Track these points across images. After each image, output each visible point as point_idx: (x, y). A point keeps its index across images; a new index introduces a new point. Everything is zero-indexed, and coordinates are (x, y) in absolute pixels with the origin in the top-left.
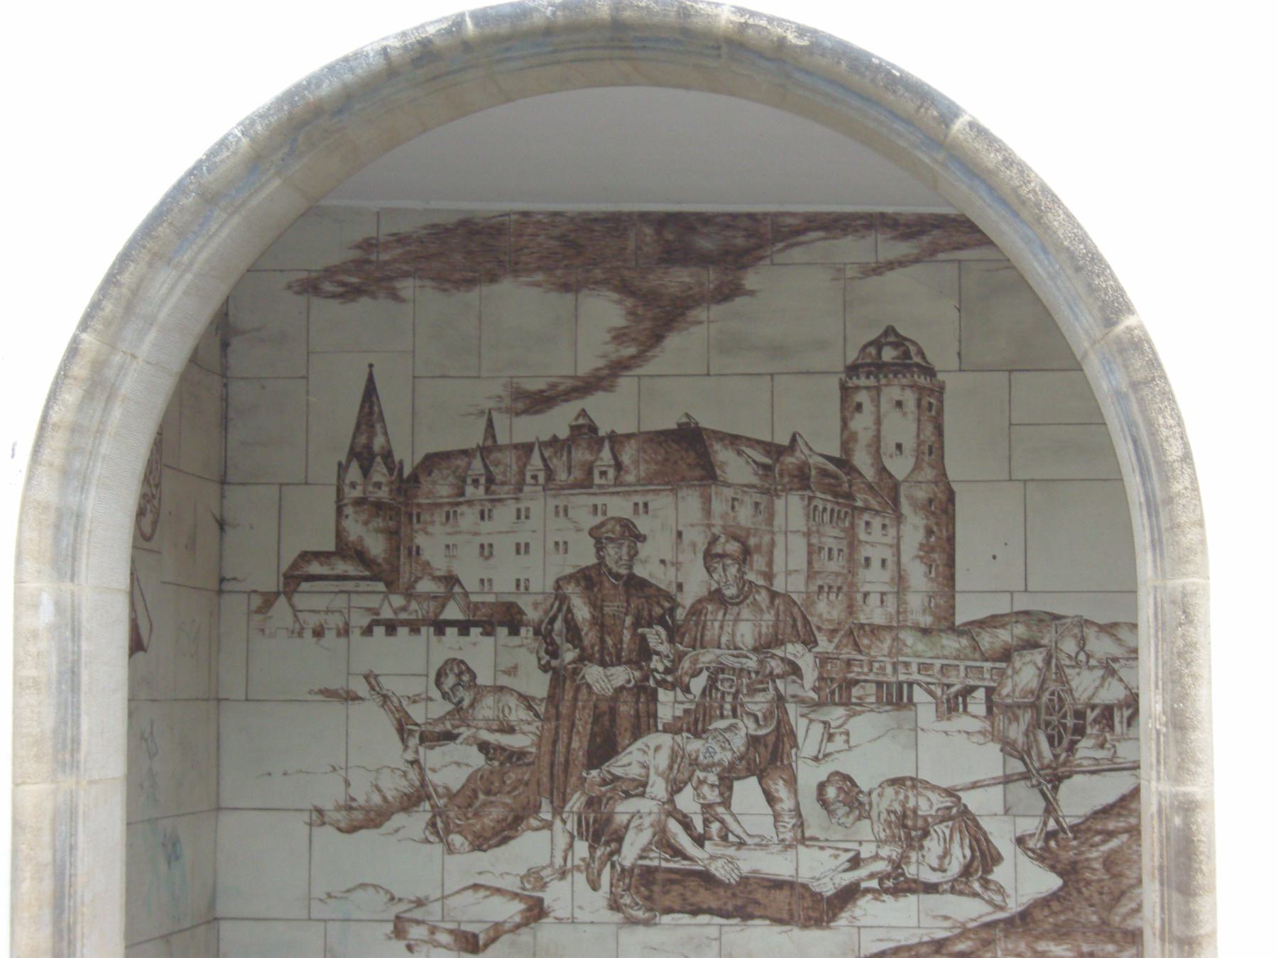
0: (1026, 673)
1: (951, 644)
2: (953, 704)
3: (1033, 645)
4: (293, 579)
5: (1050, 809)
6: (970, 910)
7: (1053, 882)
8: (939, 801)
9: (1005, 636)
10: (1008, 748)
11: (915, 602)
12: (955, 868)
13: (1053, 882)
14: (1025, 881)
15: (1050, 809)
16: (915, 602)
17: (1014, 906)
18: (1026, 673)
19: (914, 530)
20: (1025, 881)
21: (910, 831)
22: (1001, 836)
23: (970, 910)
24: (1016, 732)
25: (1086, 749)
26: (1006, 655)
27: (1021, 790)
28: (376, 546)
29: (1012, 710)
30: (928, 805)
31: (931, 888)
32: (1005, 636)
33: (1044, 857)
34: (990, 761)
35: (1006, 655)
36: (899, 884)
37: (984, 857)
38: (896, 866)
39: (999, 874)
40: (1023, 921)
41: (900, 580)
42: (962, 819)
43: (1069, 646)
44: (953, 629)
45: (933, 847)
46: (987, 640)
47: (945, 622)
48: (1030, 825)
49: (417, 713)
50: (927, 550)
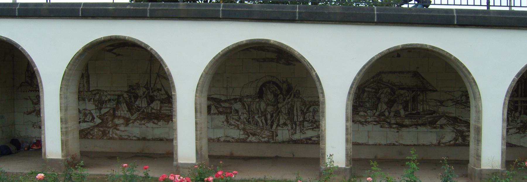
0: (97, 97)
1: (90, 93)
2: (89, 100)
3: (98, 93)
4: (21, 85)
5: (100, 113)
6: (92, 124)
7: (101, 121)
8: (89, 112)
9: (95, 92)
10: (96, 106)
11: (85, 88)
12: (90, 119)
13: (101, 121)
14: (98, 121)
15: (100, 113)
16: (85, 88)
17: (97, 124)
18: (97, 97)
19: (85, 80)
20: (98, 121)
21: (85, 115)
22: (95, 117)
23: (92, 124)
24: (96, 103)
25: (104, 106)
26: (95, 94)
27: (97, 111)
28: (29, 81)
29: (96, 101)
30: (87, 112)
31: (88, 122)
32: (95, 92)
33: (100, 118)
34: (93, 107)
35: (95, 94)
36: (85, 121)
37: (93, 118)
38: (84, 119)
39: (95, 120)
40: (98, 126)
41: (84, 86)
42: (91, 114)
43: (102, 93)
44: (90, 91)
45: (88, 117)
46: (93, 93)
47: (89, 90)
48: (98, 114)
49: (34, 101)
50: (87, 82)
